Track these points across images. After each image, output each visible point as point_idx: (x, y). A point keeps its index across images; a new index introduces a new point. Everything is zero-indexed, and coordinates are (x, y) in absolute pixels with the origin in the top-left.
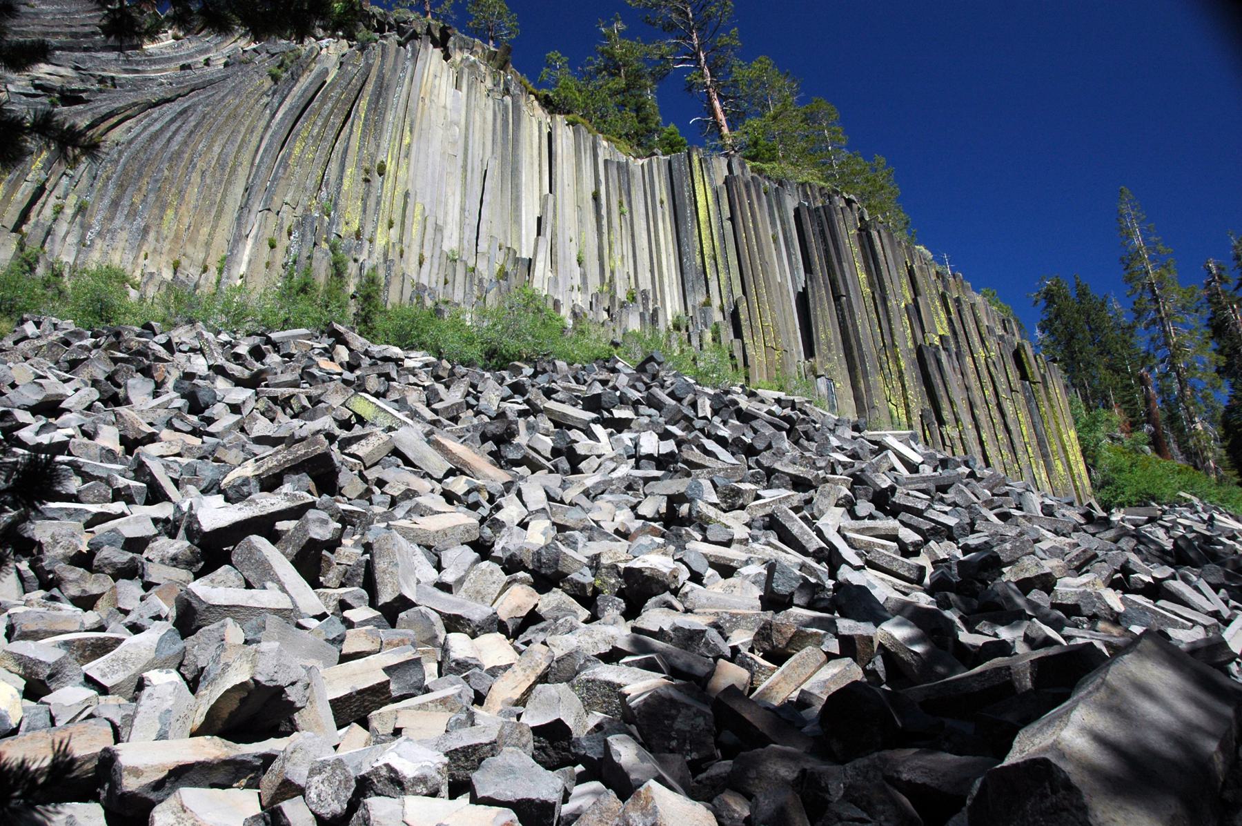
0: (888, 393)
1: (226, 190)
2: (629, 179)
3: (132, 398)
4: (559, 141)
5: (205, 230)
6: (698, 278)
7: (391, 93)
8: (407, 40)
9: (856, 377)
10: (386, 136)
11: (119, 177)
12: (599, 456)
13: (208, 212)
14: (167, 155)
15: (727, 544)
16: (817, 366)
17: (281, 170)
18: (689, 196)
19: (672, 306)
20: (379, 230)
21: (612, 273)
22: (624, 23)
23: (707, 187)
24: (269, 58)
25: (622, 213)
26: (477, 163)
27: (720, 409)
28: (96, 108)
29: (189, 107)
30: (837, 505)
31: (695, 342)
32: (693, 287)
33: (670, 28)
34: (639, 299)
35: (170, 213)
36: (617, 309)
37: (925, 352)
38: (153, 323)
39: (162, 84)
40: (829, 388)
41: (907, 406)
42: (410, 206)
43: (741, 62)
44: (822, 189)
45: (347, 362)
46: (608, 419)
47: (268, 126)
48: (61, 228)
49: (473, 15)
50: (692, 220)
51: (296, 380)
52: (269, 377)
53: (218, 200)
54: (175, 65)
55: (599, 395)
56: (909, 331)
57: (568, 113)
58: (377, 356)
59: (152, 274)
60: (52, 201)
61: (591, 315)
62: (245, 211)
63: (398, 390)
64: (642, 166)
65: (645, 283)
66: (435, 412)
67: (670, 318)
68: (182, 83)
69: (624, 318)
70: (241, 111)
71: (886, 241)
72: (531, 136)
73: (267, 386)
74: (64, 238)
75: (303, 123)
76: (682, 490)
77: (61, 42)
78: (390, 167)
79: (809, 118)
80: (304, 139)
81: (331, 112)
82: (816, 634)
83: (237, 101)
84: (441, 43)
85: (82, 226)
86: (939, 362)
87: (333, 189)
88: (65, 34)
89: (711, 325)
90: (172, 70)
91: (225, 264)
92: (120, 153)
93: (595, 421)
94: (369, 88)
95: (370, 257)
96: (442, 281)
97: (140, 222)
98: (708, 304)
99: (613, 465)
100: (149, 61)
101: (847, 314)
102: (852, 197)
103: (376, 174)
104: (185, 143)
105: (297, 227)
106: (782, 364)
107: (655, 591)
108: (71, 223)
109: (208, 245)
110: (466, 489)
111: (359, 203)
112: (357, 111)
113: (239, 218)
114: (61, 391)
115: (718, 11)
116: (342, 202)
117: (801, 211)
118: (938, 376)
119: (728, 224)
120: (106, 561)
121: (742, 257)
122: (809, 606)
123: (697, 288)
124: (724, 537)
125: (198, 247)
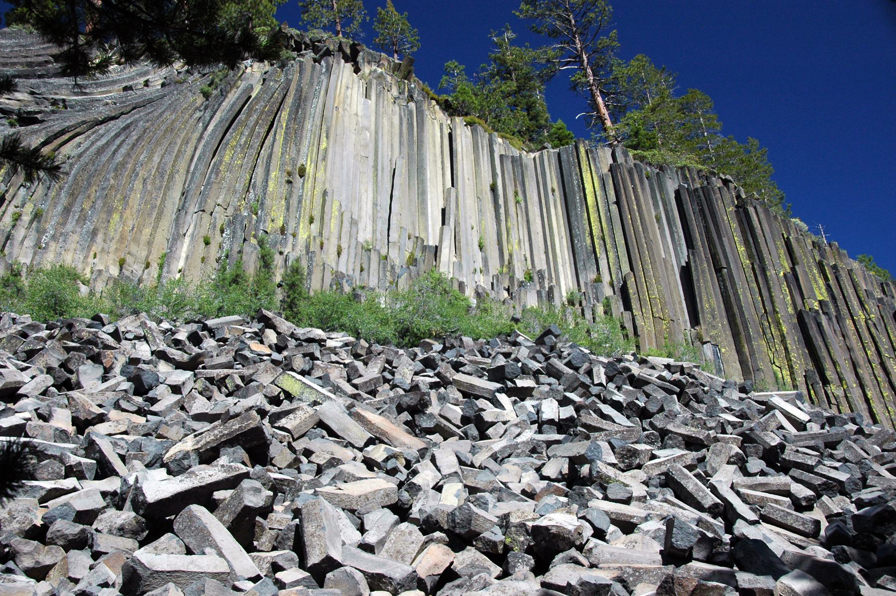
0: (771, 356)
1: (165, 194)
2: (522, 172)
3: (83, 383)
4: (459, 140)
5: (147, 231)
6: (589, 258)
7: (309, 105)
8: (322, 57)
9: (740, 342)
10: (305, 142)
11: (70, 187)
12: (504, 423)
13: (150, 215)
14: (112, 166)
15: (627, 501)
16: (703, 333)
17: (213, 176)
18: (578, 184)
19: (566, 284)
20: (301, 225)
21: (511, 255)
22: (514, 32)
23: (594, 175)
24: (201, 77)
25: (517, 202)
26: (387, 163)
27: (614, 376)
28: (50, 127)
29: (131, 123)
30: (729, 463)
31: (588, 315)
32: (585, 265)
33: (554, 34)
34: (536, 278)
35: (116, 217)
36: (516, 288)
37: (805, 317)
38: (102, 315)
39: (107, 104)
40: (715, 353)
41: (791, 368)
42: (328, 204)
43: (619, 61)
44: (699, 171)
45: (276, 344)
46: (511, 388)
47: (201, 137)
48: (20, 233)
49: (378, 33)
50: (581, 205)
51: (229, 362)
52: (206, 360)
53: (158, 204)
54: (119, 87)
55: (502, 367)
56: (789, 298)
57: (467, 114)
58: (302, 338)
59: (100, 271)
60: (11, 209)
61: (493, 295)
62: (183, 213)
63: (322, 368)
64: (534, 159)
65: (541, 264)
66: (355, 386)
67: (564, 294)
68: (125, 102)
69: (522, 295)
70: (178, 125)
71: (762, 216)
72: (434, 136)
73: (204, 368)
74: (22, 242)
75: (233, 133)
76: (583, 452)
77: (18, 71)
78: (310, 169)
79: (685, 108)
80: (233, 147)
81: (257, 123)
82: (717, 587)
83: (174, 117)
84: (352, 58)
85: (38, 231)
86: (819, 325)
87: (259, 191)
88: (21, 64)
89: (603, 300)
90: (115, 92)
91: (165, 260)
92: (72, 165)
93: (500, 391)
94: (289, 100)
95: (294, 250)
96: (358, 269)
97: (89, 226)
98: (598, 280)
99: (518, 431)
100: (95, 84)
101: (728, 284)
102: (729, 177)
103: (298, 176)
104: (128, 155)
105: (229, 225)
106: (670, 333)
107: (561, 547)
108: (28, 228)
109: (150, 243)
110: (385, 456)
111: (283, 202)
112: (279, 121)
113: (177, 220)
114: (19, 379)
115: (597, 17)
116: (268, 202)
117: (682, 191)
118: (819, 339)
119: (614, 208)
120: (58, 534)
121: (628, 237)
122: (708, 560)
123: (588, 266)
124: (623, 495)
125: (141, 246)
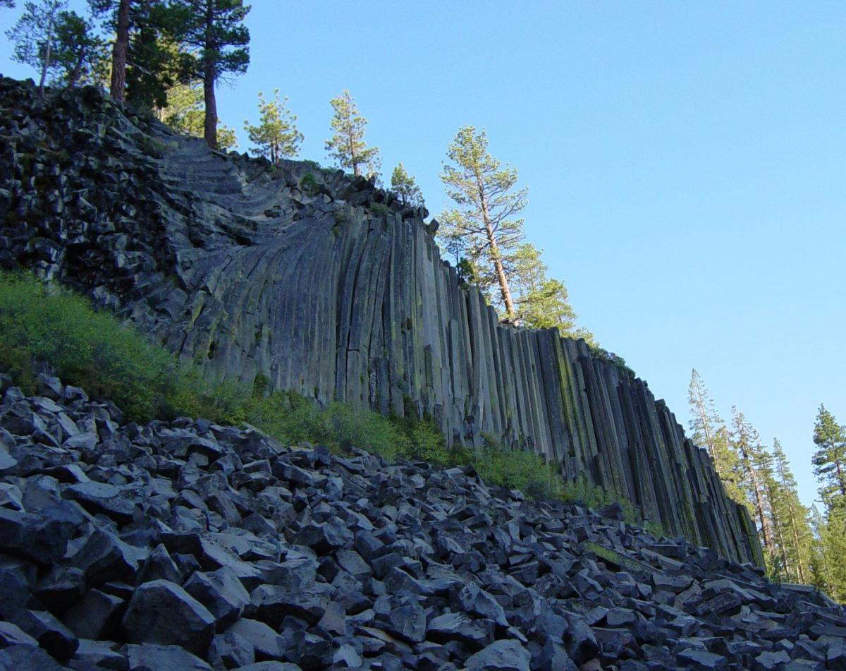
23: (568, 361)
78: (414, 324)
98: (572, 454)
100: (251, 204)
116: (394, 349)
119: (584, 394)
